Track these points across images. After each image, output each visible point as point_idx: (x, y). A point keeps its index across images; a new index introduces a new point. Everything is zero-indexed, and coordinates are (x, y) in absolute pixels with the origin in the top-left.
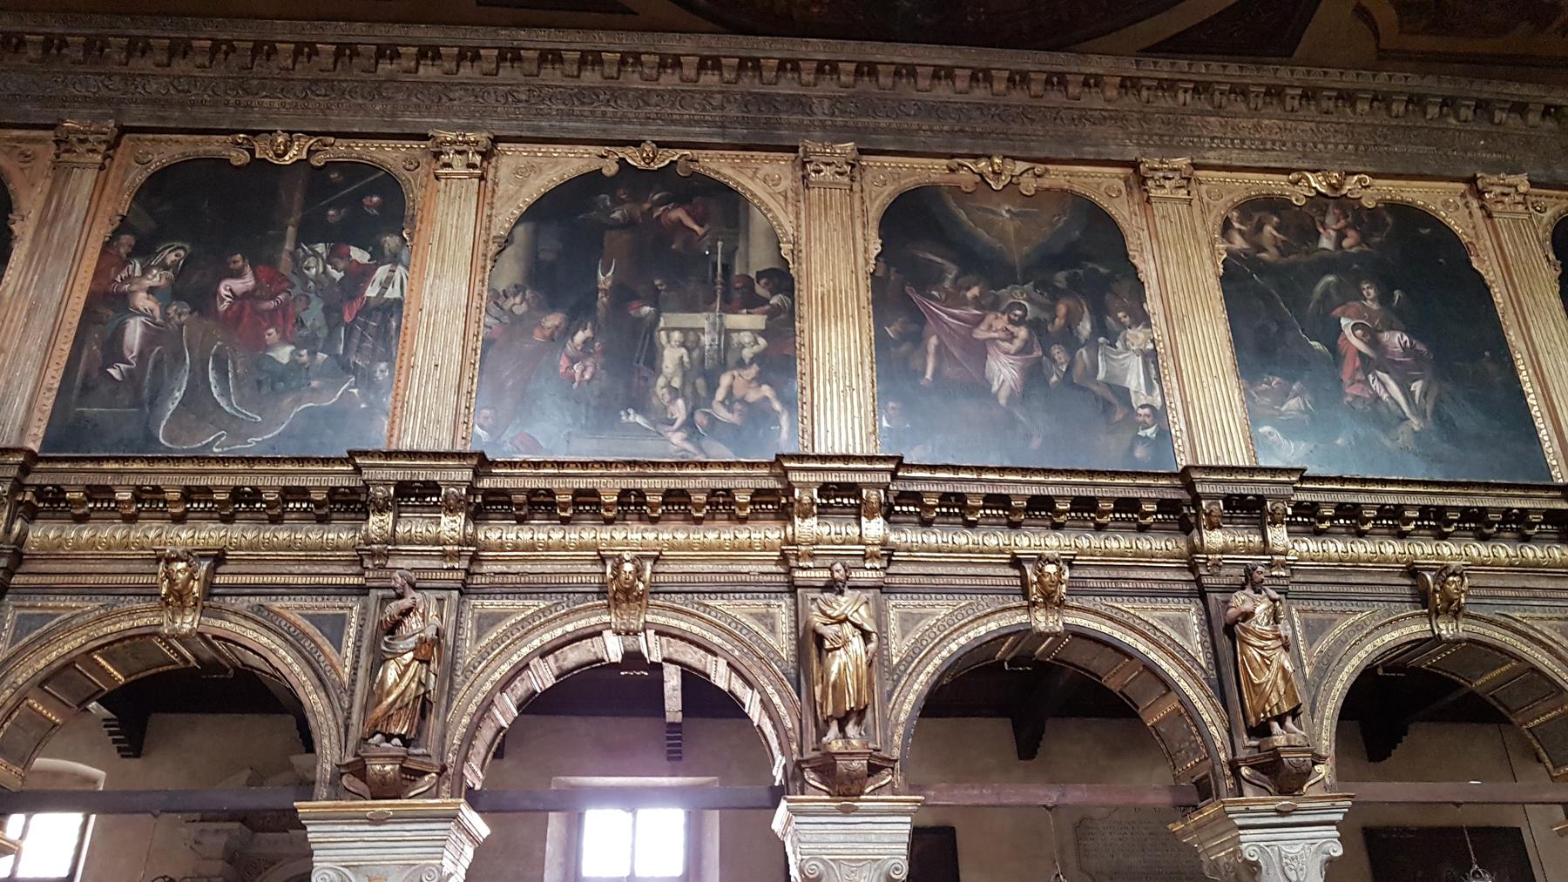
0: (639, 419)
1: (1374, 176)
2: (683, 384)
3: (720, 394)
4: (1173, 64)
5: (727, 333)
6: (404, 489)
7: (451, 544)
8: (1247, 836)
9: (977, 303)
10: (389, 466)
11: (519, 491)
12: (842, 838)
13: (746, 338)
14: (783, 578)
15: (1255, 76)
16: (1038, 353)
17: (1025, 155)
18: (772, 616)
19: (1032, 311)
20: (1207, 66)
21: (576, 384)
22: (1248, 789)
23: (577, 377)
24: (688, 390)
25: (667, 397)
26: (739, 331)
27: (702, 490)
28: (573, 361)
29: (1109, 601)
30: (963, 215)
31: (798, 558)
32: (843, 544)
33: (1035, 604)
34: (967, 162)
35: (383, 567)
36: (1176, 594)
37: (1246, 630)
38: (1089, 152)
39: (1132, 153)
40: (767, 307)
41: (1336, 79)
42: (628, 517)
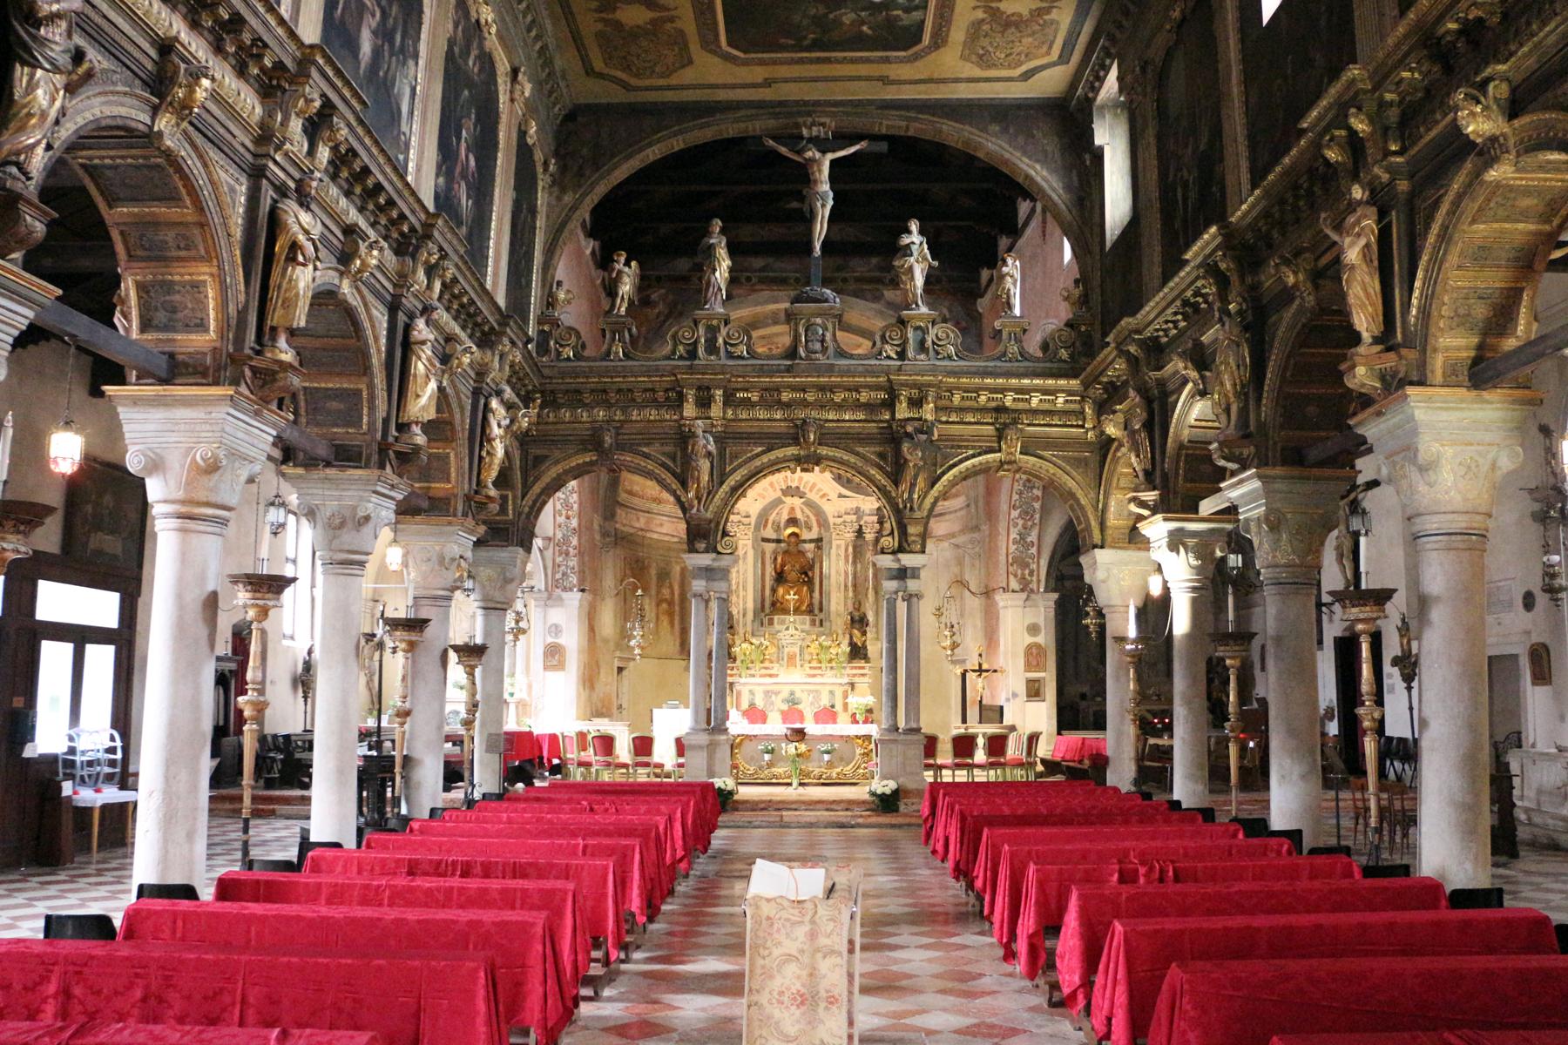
16: (380, 42)
22: (388, 467)
31: (278, 148)
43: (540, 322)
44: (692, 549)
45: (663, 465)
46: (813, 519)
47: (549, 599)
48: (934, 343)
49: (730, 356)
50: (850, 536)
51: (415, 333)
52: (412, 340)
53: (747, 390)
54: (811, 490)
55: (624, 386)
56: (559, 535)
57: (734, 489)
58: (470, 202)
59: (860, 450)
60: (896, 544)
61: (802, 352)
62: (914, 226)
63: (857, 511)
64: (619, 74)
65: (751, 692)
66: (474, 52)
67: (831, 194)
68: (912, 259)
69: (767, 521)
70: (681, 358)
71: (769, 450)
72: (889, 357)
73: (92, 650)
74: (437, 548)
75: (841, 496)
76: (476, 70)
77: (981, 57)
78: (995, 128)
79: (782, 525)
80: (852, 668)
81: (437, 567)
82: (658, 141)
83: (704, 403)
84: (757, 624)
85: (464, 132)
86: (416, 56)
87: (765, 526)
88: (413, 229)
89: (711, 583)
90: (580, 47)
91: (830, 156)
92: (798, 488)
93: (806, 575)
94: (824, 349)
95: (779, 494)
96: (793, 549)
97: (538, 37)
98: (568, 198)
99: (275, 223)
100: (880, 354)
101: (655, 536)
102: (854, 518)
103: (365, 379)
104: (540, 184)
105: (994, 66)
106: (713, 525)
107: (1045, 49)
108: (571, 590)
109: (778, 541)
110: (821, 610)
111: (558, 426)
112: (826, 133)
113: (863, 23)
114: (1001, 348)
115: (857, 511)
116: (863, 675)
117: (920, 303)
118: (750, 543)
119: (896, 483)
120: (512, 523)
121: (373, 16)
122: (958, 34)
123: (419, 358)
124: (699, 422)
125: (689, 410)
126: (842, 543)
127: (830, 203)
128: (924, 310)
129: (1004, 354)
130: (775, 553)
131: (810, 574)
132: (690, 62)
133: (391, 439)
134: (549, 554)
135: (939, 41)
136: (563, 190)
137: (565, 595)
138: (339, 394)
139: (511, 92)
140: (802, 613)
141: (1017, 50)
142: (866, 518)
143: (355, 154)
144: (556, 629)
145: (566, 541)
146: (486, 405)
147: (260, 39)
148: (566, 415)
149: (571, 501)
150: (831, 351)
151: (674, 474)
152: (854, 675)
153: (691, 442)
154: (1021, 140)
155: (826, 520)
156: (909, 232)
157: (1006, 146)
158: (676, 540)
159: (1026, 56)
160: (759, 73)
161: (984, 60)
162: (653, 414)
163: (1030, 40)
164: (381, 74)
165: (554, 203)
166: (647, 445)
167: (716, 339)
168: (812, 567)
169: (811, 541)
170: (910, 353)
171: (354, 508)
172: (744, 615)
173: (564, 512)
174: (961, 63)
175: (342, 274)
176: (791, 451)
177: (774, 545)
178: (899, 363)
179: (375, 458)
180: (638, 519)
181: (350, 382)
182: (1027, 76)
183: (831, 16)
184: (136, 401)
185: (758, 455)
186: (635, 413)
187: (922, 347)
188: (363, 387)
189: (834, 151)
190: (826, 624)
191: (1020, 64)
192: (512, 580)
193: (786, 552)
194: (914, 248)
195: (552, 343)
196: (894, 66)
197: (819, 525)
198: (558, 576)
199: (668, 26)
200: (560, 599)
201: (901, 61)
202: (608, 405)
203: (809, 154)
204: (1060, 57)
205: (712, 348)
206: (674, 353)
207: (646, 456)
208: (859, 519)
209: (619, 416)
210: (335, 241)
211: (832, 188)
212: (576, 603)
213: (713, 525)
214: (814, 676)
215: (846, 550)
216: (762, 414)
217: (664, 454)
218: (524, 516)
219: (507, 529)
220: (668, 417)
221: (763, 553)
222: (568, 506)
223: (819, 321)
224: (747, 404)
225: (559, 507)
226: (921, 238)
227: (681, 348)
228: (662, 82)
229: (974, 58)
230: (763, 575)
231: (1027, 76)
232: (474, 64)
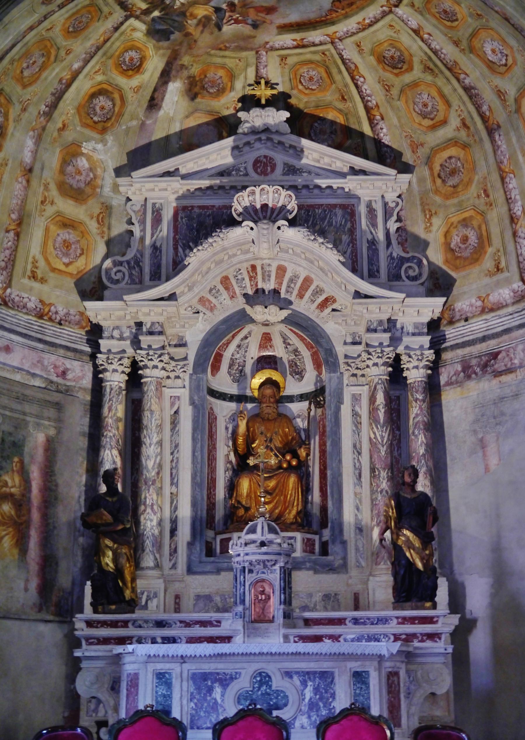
46: (306, 354)
54: (301, 296)
69: (219, 358)
75: (358, 295)
79: (248, 369)
80: (405, 620)
84: (198, 547)
87: (216, 368)
92: (276, 292)
93: (295, 455)
95: (240, 303)
96: (268, 410)
102: (385, 337)
109: (240, 399)
110: (324, 524)
116: (433, 636)
118: (184, 394)
126: (364, 391)
130: (234, 418)
131: (302, 453)
140: (286, 527)
142: (407, 340)
152: (410, 638)
155: (330, 352)
158: (38, 383)
168: (305, 443)
169: (302, 397)
172: (173, 532)
177: (233, 405)
190: (334, 548)
193: (254, 418)
197: (318, 366)
208: (395, 341)
214: (318, 639)
215: (372, 399)
221: (212, 419)
230: (212, 459)
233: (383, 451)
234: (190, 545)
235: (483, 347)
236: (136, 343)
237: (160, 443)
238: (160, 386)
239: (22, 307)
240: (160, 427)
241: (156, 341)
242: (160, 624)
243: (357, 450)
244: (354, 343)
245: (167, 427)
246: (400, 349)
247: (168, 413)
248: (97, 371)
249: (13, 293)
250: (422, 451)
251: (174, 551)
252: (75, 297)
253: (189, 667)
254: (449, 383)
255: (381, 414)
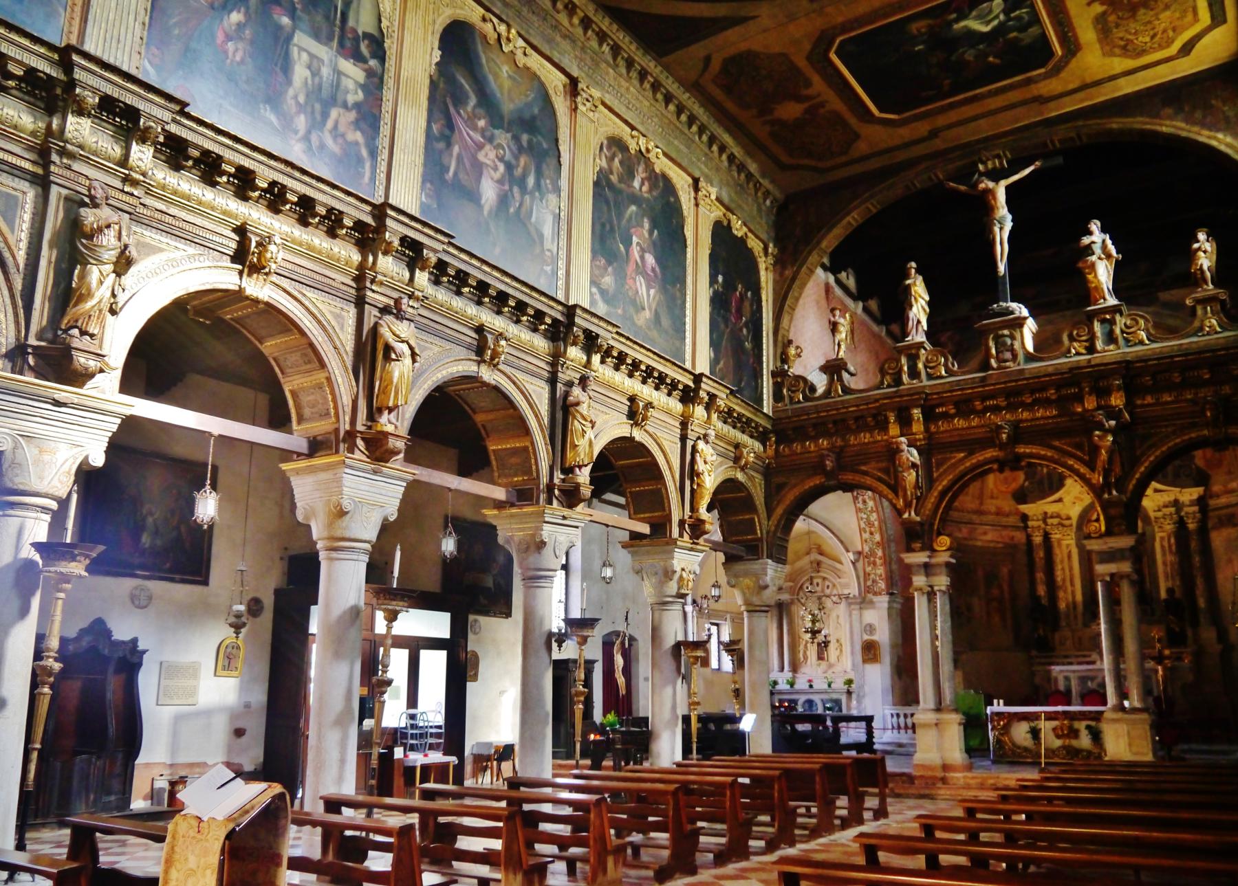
0: (273, 118)
1: (665, 154)
2: (306, 103)
3: (330, 124)
4: (611, 24)
5: (339, 73)
6: (108, 105)
7: (136, 172)
8: (546, 527)
9: (483, 132)
10: (101, 77)
11: (196, 147)
12: (367, 488)
13: (350, 85)
14: (353, 291)
15: (645, 61)
16: (507, 187)
17: (526, 36)
18: (343, 318)
19: (508, 156)
20: (624, 37)
21: (229, 61)
22: (555, 502)
23: (230, 54)
24: (309, 109)
25: (294, 109)
26: (348, 76)
27: (324, 205)
28: (229, 38)
29: (513, 371)
30: (484, 61)
31: (373, 282)
32: (398, 281)
33: (484, 361)
34: (495, 20)
35: (69, 168)
36: (539, 377)
37: (577, 411)
38: (556, 57)
39: (575, 73)
40: (366, 66)
41: (671, 85)
42: (261, 201)
43: (774, 374)
44: (910, 550)
45: (880, 480)
47: (861, 603)
48: (1123, 332)
49: (930, 377)
50: (1169, 527)
51: (571, 398)
52: (568, 403)
53: (942, 405)
55: (839, 417)
56: (866, 549)
57: (943, 494)
58: (652, 292)
59: (1057, 443)
60: (1103, 528)
61: (993, 363)
62: (1095, 226)
63: (1176, 503)
64: (806, 162)
65: (1067, 679)
66: (640, 174)
67: (1009, 217)
68: (1094, 258)
70: (889, 386)
71: (971, 453)
72: (1078, 354)
73: (425, 655)
74: (662, 563)
76: (645, 188)
77: (1124, 48)
78: (1169, 111)
81: (663, 579)
82: (855, 208)
83: (905, 422)
85: (635, 239)
86: (557, 190)
88: (555, 320)
89: (930, 578)
90: (763, 148)
91: (1004, 183)
94: (1015, 357)
97: (722, 149)
98: (788, 273)
99: (375, 330)
100: (1069, 351)
101: (979, 543)
102: (1173, 510)
103: (529, 438)
104: (762, 266)
105: (1142, 53)
106: (926, 527)
107: (1190, 17)
108: (880, 594)
111: (807, 455)
112: (1001, 163)
113: (987, 56)
114: (1197, 324)
115: (1176, 503)
117: (1107, 296)
118: (1073, 542)
119: (1093, 470)
120: (761, 540)
121: (496, 169)
122: (1087, 34)
123: (574, 417)
124: (903, 439)
125: (894, 430)
127: (1009, 225)
128: (1112, 301)
129: (1201, 329)
132: (857, 136)
133: (556, 481)
134: (860, 565)
135: (1072, 47)
136: (784, 268)
137: (875, 599)
138: (515, 452)
139: (696, 199)
141: (1160, 28)
142: (1186, 509)
143: (467, 274)
144: (870, 628)
145: (872, 553)
146: (694, 447)
147: (333, 209)
148: (797, 447)
149: (872, 519)
150: (1021, 357)
151: (889, 486)
153: (897, 457)
154: (1198, 115)
156: (1091, 233)
157: (1183, 125)
158: (1001, 545)
159: (1174, 30)
160: (923, 128)
161: (1128, 49)
162: (866, 437)
163: (1168, 13)
164: (512, 210)
165: (778, 278)
166: (865, 464)
167: (916, 365)
170: (1099, 345)
171: (533, 536)
173: (868, 529)
174: (1108, 60)
175: (479, 363)
176: (990, 453)
178: (1088, 357)
179: (543, 497)
180: (960, 530)
181: (519, 442)
182: (1187, 49)
183: (953, 58)
184: (297, 472)
185: (962, 461)
186: (852, 438)
187: (1111, 338)
188: (528, 444)
189: (1007, 177)
191: (1170, 42)
192: (766, 587)
194: (1097, 248)
195: (785, 391)
196: (1042, 84)
198: (869, 583)
199: (822, 111)
200: (871, 602)
201: (1047, 76)
202: (827, 434)
203: (982, 186)
204: (1213, 17)
205: (914, 374)
206: (882, 383)
207: (865, 473)
209: (839, 442)
210: (469, 340)
211: (1009, 211)
212: (886, 605)
213: (926, 527)
216: (959, 423)
217: (880, 470)
218: (771, 534)
219: (757, 546)
220: (879, 438)
222: (870, 524)
223: (1006, 332)
224: (946, 416)
225: (863, 525)
226: (1103, 236)
227: (888, 377)
228: (844, 159)
229: (1117, 51)
231: (1187, 49)
232: (642, 184)
233: (1176, 567)
234: (1084, 614)
235: (1224, 512)
236: (1044, 521)
237: (1063, 569)
238: (1059, 541)
239: (990, 513)
240: (1062, 562)
241: (1055, 521)
242: (1066, 657)
243: (1165, 563)
244: (1159, 510)
245: (1066, 559)
246: (1183, 514)
247: (1065, 552)
248: (1029, 537)
249: (984, 508)
250: (1198, 565)
251: (1076, 617)
252: (1012, 502)
253: (1077, 674)
254: (1215, 528)
255: (1174, 548)
